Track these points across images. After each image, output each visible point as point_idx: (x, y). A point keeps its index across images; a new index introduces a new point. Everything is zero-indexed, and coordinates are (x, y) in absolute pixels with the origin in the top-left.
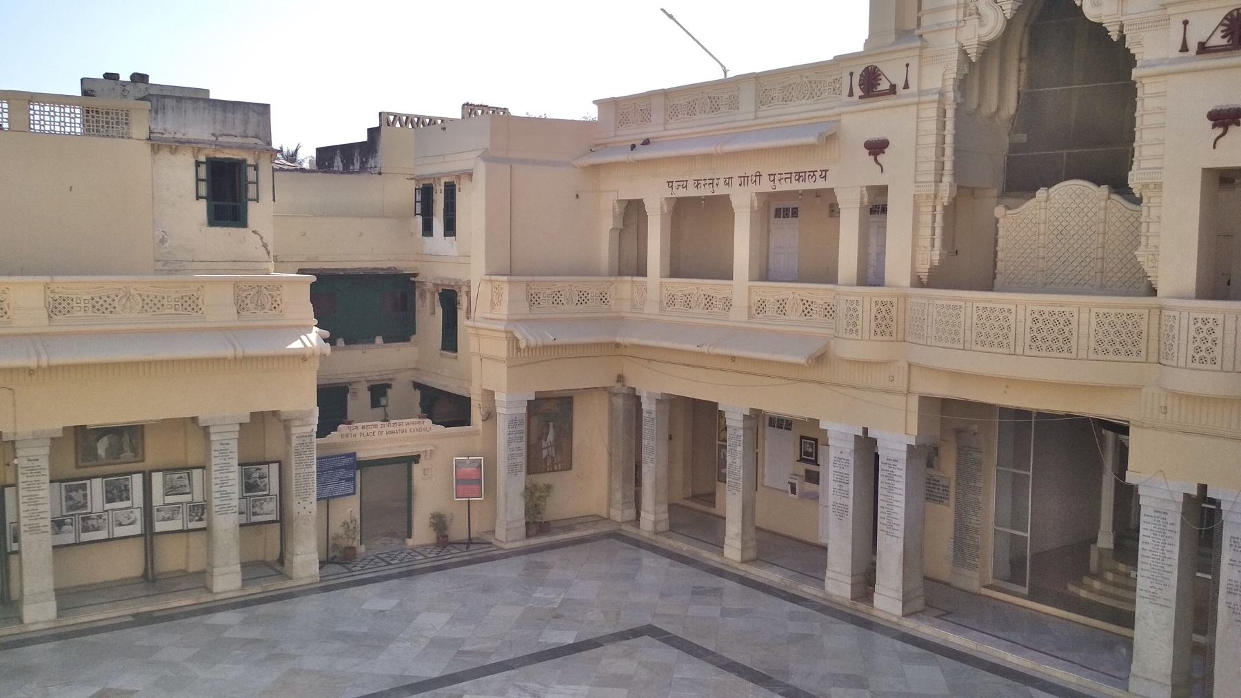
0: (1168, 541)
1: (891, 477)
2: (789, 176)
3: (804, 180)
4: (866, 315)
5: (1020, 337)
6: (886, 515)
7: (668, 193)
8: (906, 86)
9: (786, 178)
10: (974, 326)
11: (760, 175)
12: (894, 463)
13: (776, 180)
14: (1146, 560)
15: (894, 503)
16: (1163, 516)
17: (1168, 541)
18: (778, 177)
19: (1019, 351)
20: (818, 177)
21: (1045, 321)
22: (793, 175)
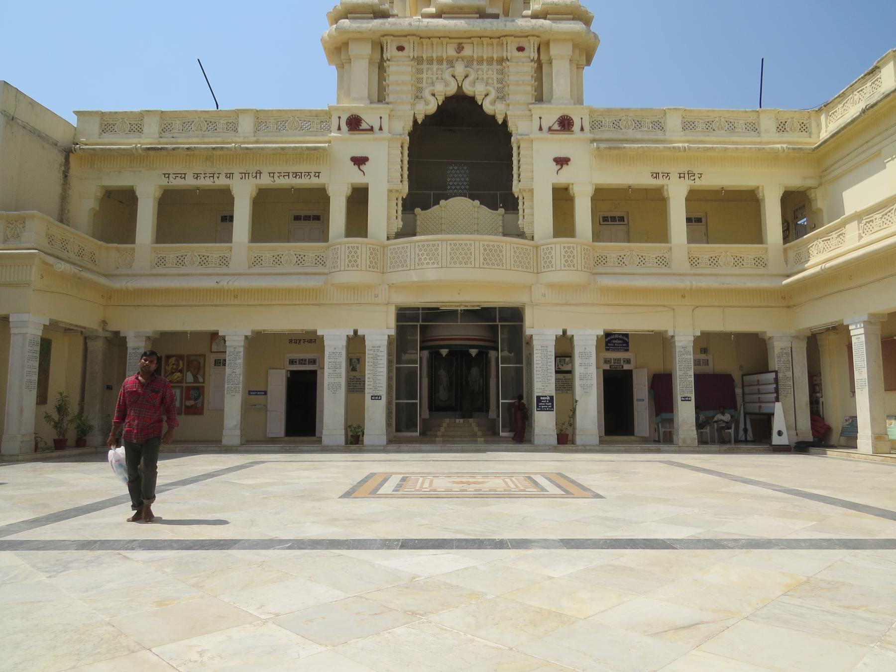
0: (549, 360)
1: (375, 358)
2: (288, 174)
4: (364, 256)
5: (477, 257)
6: (372, 383)
7: (164, 182)
8: (381, 129)
10: (448, 254)
12: (378, 348)
14: (538, 373)
15: (378, 374)
16: (546, 348)
17: (549, 360)
19: (477, 265)
20: (312, 176)
21: (491, 250)
22: (291, 175)
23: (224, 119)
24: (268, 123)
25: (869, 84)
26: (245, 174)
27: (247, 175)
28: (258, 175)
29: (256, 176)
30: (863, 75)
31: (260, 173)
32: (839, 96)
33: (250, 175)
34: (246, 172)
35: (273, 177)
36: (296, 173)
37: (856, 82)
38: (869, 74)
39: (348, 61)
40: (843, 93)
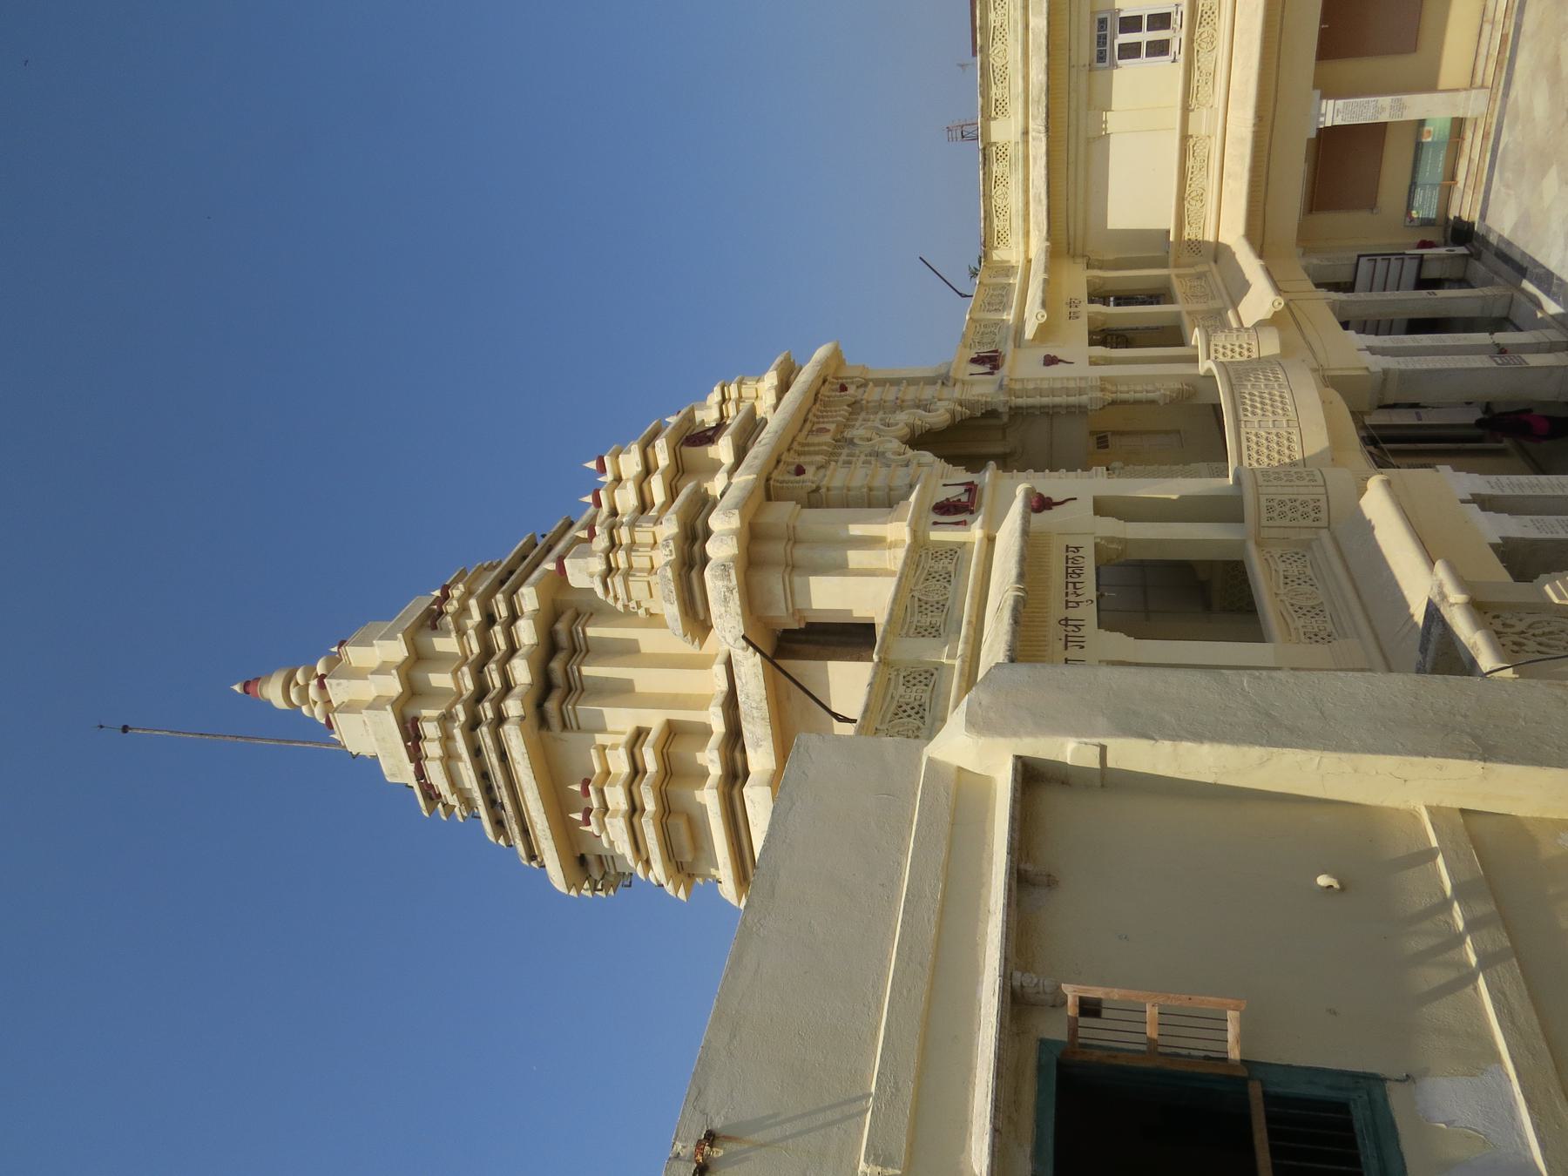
2: (1071, 586)
3: (1081, 568)
9: (1075, 588)
11: (1066, 619)
13: (1078, 599)
18: (1072, 598)
20: (1078, 554)
22: (1070, 580)
23: (891, 689)
24: (919, 624)
25: (995, 168)
26: (1067, 641)
27: (1069, 639)
28: (1070, 623)
29: (1075, 626)
30: (981, 173)
31: (1066, 619)
32: (985, 219)
33: (1069, 634)
34: (1063, 641)
35: (1077, 603)
36: (1067, 573)
37: (984, 186)
38: (985, 164)
39: (791, 542)
40: (985, 211)
